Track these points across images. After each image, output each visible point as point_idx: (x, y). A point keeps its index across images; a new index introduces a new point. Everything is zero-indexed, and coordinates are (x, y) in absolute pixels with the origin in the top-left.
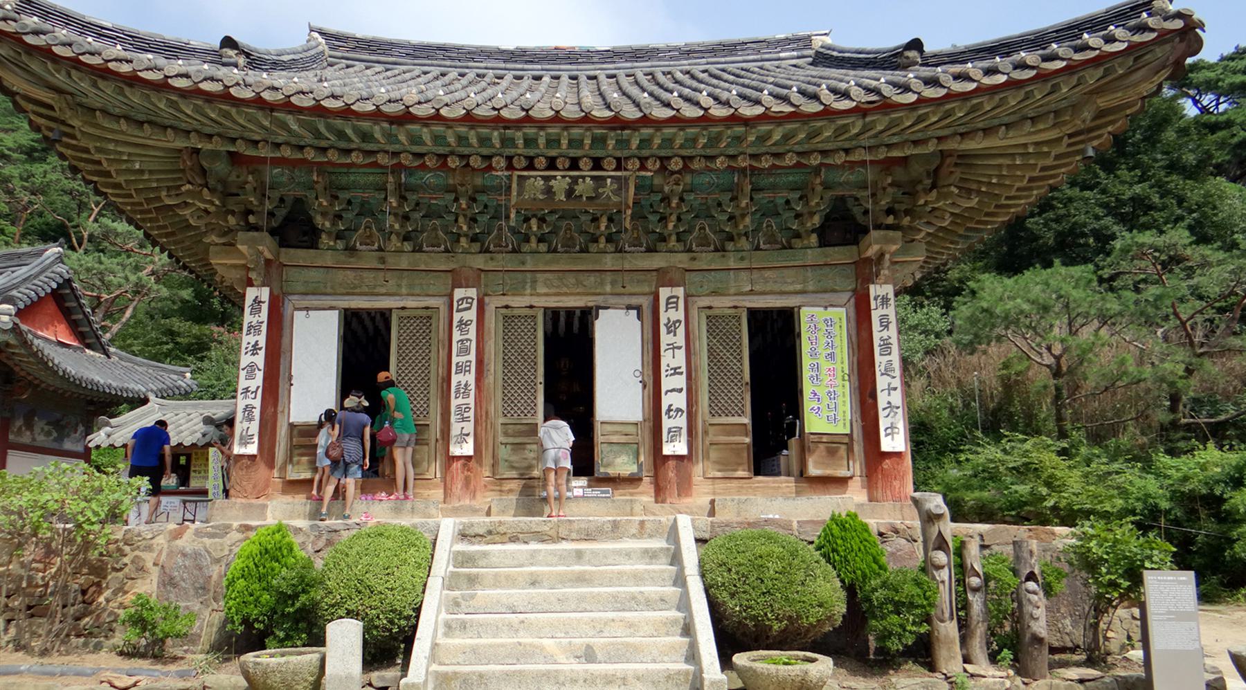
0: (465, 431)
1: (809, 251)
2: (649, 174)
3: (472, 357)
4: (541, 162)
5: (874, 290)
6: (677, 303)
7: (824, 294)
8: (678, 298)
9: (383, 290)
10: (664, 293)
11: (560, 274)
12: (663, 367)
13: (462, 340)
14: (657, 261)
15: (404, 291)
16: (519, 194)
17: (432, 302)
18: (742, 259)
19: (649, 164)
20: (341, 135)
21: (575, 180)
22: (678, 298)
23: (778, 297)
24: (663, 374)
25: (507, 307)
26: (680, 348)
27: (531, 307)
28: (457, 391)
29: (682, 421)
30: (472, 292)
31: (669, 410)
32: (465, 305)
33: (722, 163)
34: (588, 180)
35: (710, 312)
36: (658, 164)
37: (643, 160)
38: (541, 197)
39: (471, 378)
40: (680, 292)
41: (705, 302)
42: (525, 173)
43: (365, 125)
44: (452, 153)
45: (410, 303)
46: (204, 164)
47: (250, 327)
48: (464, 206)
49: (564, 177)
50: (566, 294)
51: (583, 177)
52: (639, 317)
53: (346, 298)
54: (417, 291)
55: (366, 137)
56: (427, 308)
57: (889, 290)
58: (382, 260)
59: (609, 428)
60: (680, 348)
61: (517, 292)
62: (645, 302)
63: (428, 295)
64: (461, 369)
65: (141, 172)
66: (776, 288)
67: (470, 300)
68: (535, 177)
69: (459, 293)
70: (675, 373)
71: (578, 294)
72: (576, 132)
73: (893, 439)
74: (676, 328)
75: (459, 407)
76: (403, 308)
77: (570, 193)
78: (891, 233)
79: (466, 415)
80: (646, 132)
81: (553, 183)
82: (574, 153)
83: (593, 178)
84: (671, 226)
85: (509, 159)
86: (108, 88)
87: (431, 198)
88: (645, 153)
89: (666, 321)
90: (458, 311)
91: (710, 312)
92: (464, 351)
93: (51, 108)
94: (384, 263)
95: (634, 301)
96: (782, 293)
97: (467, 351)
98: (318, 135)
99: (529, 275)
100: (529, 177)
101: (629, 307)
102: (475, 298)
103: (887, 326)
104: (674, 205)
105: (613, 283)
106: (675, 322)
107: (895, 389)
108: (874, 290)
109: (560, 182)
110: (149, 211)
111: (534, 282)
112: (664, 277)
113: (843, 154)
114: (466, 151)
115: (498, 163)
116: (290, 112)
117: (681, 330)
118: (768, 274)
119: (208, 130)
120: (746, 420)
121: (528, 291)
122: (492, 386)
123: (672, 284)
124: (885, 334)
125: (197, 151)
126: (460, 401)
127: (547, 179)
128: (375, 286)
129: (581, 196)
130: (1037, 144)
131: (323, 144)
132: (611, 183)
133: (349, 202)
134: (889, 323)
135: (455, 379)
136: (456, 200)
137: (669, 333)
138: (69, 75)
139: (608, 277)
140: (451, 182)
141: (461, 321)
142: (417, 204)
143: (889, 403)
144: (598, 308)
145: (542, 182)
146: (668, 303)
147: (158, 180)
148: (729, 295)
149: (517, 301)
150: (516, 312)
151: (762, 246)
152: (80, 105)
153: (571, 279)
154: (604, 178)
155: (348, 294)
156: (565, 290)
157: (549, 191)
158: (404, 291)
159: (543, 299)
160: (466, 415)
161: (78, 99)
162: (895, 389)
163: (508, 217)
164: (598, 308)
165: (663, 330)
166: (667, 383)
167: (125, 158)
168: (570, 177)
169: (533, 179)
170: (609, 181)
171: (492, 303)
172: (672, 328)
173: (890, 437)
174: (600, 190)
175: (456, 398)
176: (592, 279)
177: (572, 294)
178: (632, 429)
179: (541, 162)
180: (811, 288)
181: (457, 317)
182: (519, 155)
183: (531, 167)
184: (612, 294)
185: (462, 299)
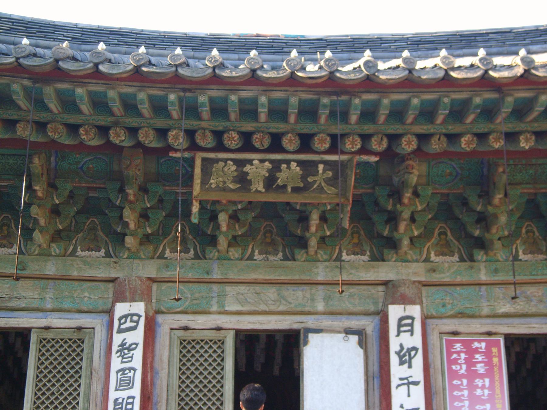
2: (374, 159)
3: (136, 391)
6: (412, 325)
8: (413, 319)
11: (258, 288)
13: (123, 370)
17: (84, 320)
18: (496, 271)
21: (276, 165)
22: (413, 319)
25: (186, 329)
26: (416, 383)
27: (219, 329)
30: (139, 308)
32: (129, 324)
33: (468, 143)
34: (294, 165)
36: (385, 144)
37: (365, 138)
38: (232, 186)
40: (415, 311)
42: (212, 155)
44: (116, 124)
48: (131, 198)
49: (262, 161)
51: (288, 162)
52: (362, 343)
54: (67, 305)
60: (416, 383)
63: (80, 311)
67: (135, 318)
68: (225, 161)
69: (121, 309)
74: (411, 358)
76: (47, 328)
83: (300, 163)
84: (402, 227)
85: (190, 134)
87: (89, 189)
88: (368, 128)
89: (398, 349)
90: (120, 331)
95: (355, 323)
97: (129, 384)
99: (215, 287)
100: (217, 161)
101: (348, 332)
102: (143, 314)
104: (406, 201)
105: (327, 299)
106: (409, 350)
111: (222, 296)
114: (133, 122)
117: (418, 361)
118: (530, 290)
121: (215, 308)
123: (405, 301)
127: (240, 163)
129: (284, 187)
132: (324, 171)
136: (122, 190)
137: (402, 363)
139: (320, 291)
140: (116, 167)
141: (123, 345)
142: (71, 196)
145: (234, 168)
146: (400, 325)
148: (480, 317)
150: (197, 335)
153: (271, 293)
154: (314, 164)
163: (187, 214)
165: (394, 359)
168: (271, 161)
169: (221, 164)
170: (321, 167)
174: (310, 179)
176: (300, 294)
181: (117, 339)
182: (204, 129)
183: (220, 147)
184: (325, 313)
185: (126, 316)
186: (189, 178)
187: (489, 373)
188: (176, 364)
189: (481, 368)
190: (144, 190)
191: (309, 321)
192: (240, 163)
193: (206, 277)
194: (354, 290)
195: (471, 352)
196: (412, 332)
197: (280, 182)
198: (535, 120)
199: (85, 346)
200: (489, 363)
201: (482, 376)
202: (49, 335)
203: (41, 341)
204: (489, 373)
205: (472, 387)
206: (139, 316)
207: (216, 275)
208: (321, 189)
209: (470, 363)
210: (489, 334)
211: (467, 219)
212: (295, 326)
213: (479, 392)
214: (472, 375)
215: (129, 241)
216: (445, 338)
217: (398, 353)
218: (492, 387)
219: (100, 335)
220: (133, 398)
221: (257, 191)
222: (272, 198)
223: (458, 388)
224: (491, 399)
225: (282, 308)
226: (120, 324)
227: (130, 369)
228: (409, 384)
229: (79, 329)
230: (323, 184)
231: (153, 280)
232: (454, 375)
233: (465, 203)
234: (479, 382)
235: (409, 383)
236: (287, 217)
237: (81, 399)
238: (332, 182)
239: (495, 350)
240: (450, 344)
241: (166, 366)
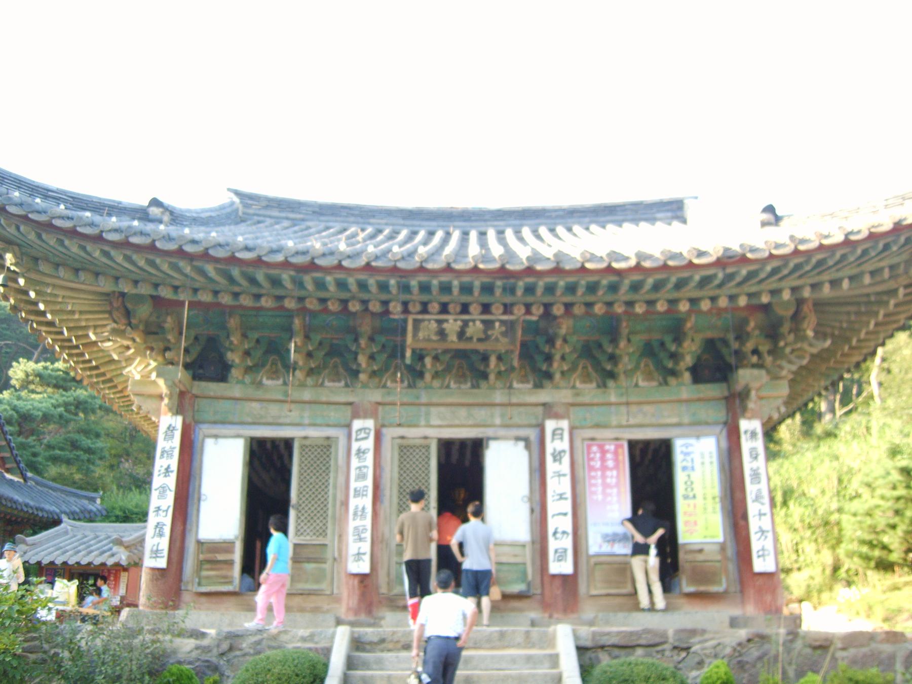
4: (434, 307)
6: (562, 434)
7: (697, 427)
8: (562, 429)
9: (288, 421)
11: (453, 408)
13: (360, 468)
14: (544, 396)
19: (534, 309)
20: (253, 281)
21: (466, 323)
25: (402, 438)
26: (564, 475)
27: (426, 438)
28: (355, 514)
30: (370, 423)
31: (555, 533)
32: (363, 435)
33: (600, 309)
34: (478, 323)
36: (541, 310)
40: (565, 424)
42: (420, 317)
43: (274, 272)
44: (353, 298)
45: (313, 433)
46: (129, 306)
47: (163, 452)
49: (455, 320)
51: (474, 321)
52: (528, 447)
53: (253, 427)
54: (319, 421)
55: (276, 282)
58: (286, 394)
60: (564, 475)
62: (532, 434)
63: (328, 425)
64: (357, 493)
65: (72, 312)
66: (654, 421)
67: (367, 431)
68: (429, 320)
69: (357, 424)
72: (466, 279)
73: (764, 560)
75: (356, 528)
76: (305, 438)
77: (461, 334)
80: (530, 280)
81: (445, 325)
82: (465, 299)
84: (555, 365)
85: (405, 304)
86: (51, 240)
87: (333, 339)
88: (529, 299)
90: (357, 440)
92: (361, 477)
95: (522, 432)
98: (231, 280)
99: (423, 409)
100: (423, 320)
101: (518, 439)
103: (756, 458)
105: (502, 416)
106: (560, 453)
107: (765, 514)
108: (745, 425)
109: (452, 325)
110: (77, 347)
111: (428, 414)
112: (550, 411)
114: (365, 296)
115: (395, 307)
116: (208, 262)
117: (566, 459)
118: (646, 408)
119: (134, 277)
123: (557, 416)
124: (755, 465)
125: (123, 295)
126: (358, 523)
127: (440, 322)
128: (279, 417)
130: (878, 294)
131: (237, 289)
132: (500, 326)
136: (356, 340)
138: (18, 228)
139: (497, 411)
142: (320, 344)
143: (760, 527)
144: (489, 439)
147: (87, 320)
150: (411, 442)
153: (463, 412)
155: (254, 423)
157: (442, 334)
161: (24, 250)
162: (765, 514)
163: (403, 356)
164: (489, 439)
165: (549, 459)
167: (60, 300)
168: (463, 321)
169: (426, 323)
170: (497, 324)
171: (389, 433)
172: (557, 457)
173: (761, 559)
174: (490, 333)
175: (354, 519)
179: (434, 307)
181: (355, 446)
185: (360, 430)
186: (404, 331)
187: (616, 467)
188: (396, 463)
189: (610, 464)
190: (371, 339)
191: (489, 432)
192: (440, 322)
193: (417, 401)
194: (522, 409)
195: (604, 452)
196: (562, 439)
197: (468, 335)
198: (647, 292)
199: (333, 450)
200: (616, 460)
201: (611, 469)
202: (307, 442)
203: (303, 447)
204: (616, 467)
205: (604, 477)
206: (370, 430)
207: (424, 399)
208: (497, 340)
209: (603, 459)
210: (617, 439)
211: (602, 358)
212: (480, 436)
213: (608, 480)
214: (604, 468)
215: (362, 377)
216: (586, 443)
218: (618, 477)
220: (366, 487)
221: (452, 342)
222: (463, 346)
223: (594, 477)
224: (617, 485)
225: (470, 422)
226: (357, 435)
227: (365, 467)
228: (559, 476)
229: (328, 438)
230: (499, 336)
231: (379, 404)
232: (592, 468)
233: (600, 346)
234: (609, 473)
235: (559, 475)
236: (474, 358)
237: (331, 487)
238: (504, 334)
239: (620, 451)
240: (589, 447)
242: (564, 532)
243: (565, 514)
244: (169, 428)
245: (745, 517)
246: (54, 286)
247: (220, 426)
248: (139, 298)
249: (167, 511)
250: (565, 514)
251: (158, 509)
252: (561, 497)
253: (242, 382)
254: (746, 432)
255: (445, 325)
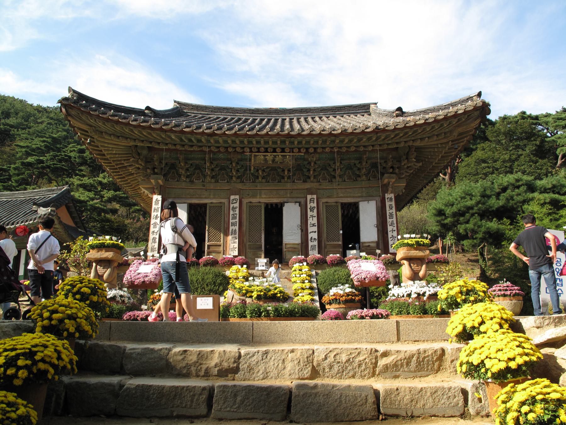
0: (235, 247)
1: (363, 182)
2: (302, 154)
3: (237, 220)
4: (262, 149)
5: (387, 196)
6: (314, 200)
7: (368, 198)
8: (314, 199)
10: (309, 197)
12: (309, 224)
13: (233, 214)
14: (307, 185)
15: (212, 197)
16: (255, 161)
19: (302, 150)
20: (190, 140)
21: (275, 156)
22: (314, 199)
23: (352, 198)
24: (309, 226)
26: (315, 217)
27: (260, 202)
28: (232, 233)
29: (316, 243)
32: (234, 201)
35: (326, 204)
36: (305, 150)
37: (299, 149)
38: (263, 162)
39: (237, 228)
40: (315, 196)
41: (325, 200)
42: (257, 154)
43: (199, 137)
46: (139, 151)
47: (155, 209)
48: (234, 166)
50: (272, 198)
51: (278, 155)
54: (216, 197)
55: (199, 141)
56: (221, 203)
57: (392, 196)
59: (288, 246)
60: (315, 217)
61: (254, 196)
64: (233, 224)
65: (116, 154)
68: (261, 155)
69: (232, 197)
70: (313, 226)
71: (277, 198)
72: (274, 139)
76: (211, 203)
77: (273, 161)
78: (392, 175)
79: (235, 241)
80: (300, 139)
81: (267, 157)
82: (274, 146)
83: (282, 155)
84: (311, 172)
85: (251, 148)
86: (109, 125)
88: (300, 146)
90: (232, 203)
91: (326, 204)
92: (234, 218)
93: (87, 132)
94: (204, 186)
95: (298, 200)
96: (353, 197)
97: (235, 218)
98: (181, 140)
99: (258, 191)
100: (258, 155)
101: (296, 202)
103: (392, 209)
104: (312, 165)
106: (313, 208)
108: (387, 196)
113: (371, 147)
114: (235, 146)
115: (247, 150)
116: (172, 133)
117: (315, 210)
118: (348, 190)
119: (142, 139)
120: (340, 243)
121: (258, 197)
122: (245, 231)
123: (312, 194)
124: (391, 211)
125: (136, 146)
131: (183, 143)
133: (191, 165)
134: (392, 207)
135: (231, 228)
136: (231, 163)
137: (311, 211)
138: (95, 121)
140: (229, 157)
141: (233, 207)
149: (254, 200)
150: (254, 204)
151: (346, 180)
152: (97, 130)
154: (286, 156)
155: (190, 198)
156: (272, 196)
157: (266, 160)
158: (212, 197)
159: (264, 199)
160: (235, 241)
161: (97, 129)
163: (250, 170)
165: (309, 210)
166: (310, 229)
168: (273, 155)
170: (288, 156)
171: (245, 201)
177: (275, 198)
178: (296, 246)
179: (262, 149)
180: (364, 195)
181: (231, 206)
182: (254, 147)
183: (259, 152)
184: (290, 198)
185: (234, 199)
186: (250, 160)
190: (238, 163)
192: (265, 156)
198: (347, 143)
203: (210, 207)
215: (234, 179)
217: (310, 208)
219: (226, 204)
222: (274, 165)
227: (235, 214)
228: (313, 217)
235: (312, 216)
236: (279, 170)
241: (245, 213)
242: (315, 239)
243: (315, 232)
244: (156, 200)
245: (387, 233)
246: (108, 143)
247: (177, 199)
248: (143, 148)
249: (157, 233)
250: (315, 232)
251: (154, 232)
252: (314, 225)
253: (185, 181)
254: (388, 198)
255: (267, 157)
